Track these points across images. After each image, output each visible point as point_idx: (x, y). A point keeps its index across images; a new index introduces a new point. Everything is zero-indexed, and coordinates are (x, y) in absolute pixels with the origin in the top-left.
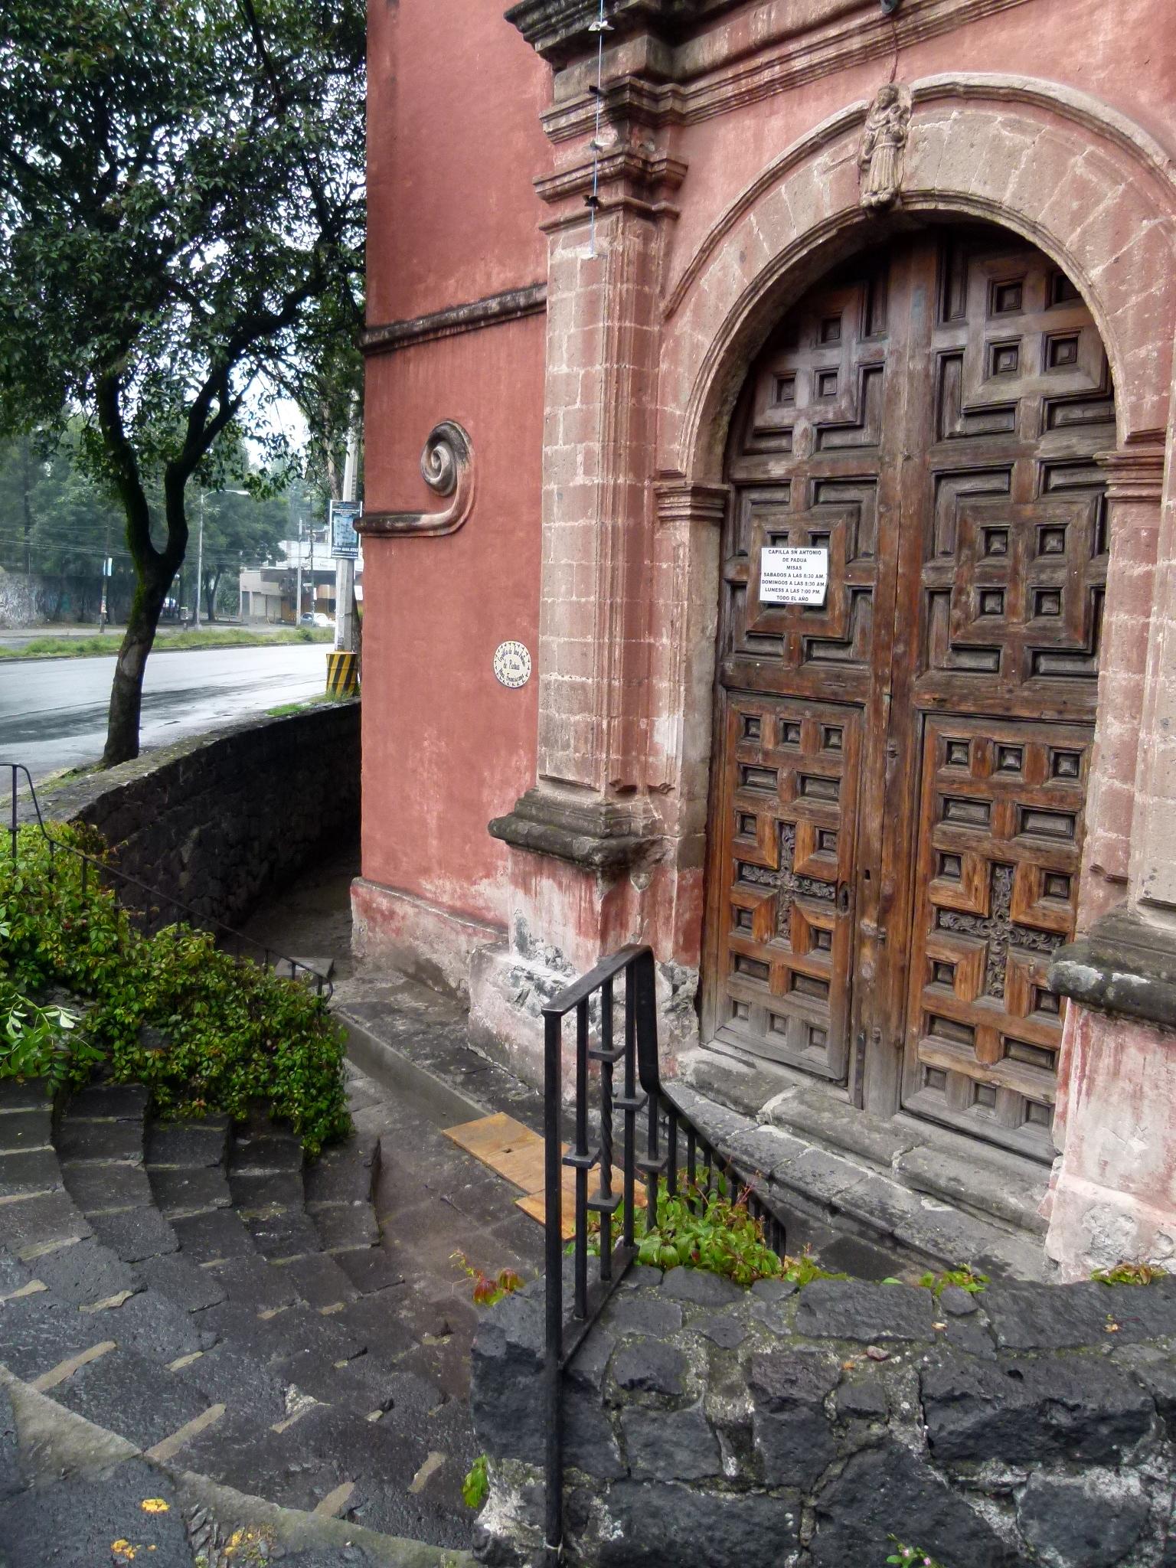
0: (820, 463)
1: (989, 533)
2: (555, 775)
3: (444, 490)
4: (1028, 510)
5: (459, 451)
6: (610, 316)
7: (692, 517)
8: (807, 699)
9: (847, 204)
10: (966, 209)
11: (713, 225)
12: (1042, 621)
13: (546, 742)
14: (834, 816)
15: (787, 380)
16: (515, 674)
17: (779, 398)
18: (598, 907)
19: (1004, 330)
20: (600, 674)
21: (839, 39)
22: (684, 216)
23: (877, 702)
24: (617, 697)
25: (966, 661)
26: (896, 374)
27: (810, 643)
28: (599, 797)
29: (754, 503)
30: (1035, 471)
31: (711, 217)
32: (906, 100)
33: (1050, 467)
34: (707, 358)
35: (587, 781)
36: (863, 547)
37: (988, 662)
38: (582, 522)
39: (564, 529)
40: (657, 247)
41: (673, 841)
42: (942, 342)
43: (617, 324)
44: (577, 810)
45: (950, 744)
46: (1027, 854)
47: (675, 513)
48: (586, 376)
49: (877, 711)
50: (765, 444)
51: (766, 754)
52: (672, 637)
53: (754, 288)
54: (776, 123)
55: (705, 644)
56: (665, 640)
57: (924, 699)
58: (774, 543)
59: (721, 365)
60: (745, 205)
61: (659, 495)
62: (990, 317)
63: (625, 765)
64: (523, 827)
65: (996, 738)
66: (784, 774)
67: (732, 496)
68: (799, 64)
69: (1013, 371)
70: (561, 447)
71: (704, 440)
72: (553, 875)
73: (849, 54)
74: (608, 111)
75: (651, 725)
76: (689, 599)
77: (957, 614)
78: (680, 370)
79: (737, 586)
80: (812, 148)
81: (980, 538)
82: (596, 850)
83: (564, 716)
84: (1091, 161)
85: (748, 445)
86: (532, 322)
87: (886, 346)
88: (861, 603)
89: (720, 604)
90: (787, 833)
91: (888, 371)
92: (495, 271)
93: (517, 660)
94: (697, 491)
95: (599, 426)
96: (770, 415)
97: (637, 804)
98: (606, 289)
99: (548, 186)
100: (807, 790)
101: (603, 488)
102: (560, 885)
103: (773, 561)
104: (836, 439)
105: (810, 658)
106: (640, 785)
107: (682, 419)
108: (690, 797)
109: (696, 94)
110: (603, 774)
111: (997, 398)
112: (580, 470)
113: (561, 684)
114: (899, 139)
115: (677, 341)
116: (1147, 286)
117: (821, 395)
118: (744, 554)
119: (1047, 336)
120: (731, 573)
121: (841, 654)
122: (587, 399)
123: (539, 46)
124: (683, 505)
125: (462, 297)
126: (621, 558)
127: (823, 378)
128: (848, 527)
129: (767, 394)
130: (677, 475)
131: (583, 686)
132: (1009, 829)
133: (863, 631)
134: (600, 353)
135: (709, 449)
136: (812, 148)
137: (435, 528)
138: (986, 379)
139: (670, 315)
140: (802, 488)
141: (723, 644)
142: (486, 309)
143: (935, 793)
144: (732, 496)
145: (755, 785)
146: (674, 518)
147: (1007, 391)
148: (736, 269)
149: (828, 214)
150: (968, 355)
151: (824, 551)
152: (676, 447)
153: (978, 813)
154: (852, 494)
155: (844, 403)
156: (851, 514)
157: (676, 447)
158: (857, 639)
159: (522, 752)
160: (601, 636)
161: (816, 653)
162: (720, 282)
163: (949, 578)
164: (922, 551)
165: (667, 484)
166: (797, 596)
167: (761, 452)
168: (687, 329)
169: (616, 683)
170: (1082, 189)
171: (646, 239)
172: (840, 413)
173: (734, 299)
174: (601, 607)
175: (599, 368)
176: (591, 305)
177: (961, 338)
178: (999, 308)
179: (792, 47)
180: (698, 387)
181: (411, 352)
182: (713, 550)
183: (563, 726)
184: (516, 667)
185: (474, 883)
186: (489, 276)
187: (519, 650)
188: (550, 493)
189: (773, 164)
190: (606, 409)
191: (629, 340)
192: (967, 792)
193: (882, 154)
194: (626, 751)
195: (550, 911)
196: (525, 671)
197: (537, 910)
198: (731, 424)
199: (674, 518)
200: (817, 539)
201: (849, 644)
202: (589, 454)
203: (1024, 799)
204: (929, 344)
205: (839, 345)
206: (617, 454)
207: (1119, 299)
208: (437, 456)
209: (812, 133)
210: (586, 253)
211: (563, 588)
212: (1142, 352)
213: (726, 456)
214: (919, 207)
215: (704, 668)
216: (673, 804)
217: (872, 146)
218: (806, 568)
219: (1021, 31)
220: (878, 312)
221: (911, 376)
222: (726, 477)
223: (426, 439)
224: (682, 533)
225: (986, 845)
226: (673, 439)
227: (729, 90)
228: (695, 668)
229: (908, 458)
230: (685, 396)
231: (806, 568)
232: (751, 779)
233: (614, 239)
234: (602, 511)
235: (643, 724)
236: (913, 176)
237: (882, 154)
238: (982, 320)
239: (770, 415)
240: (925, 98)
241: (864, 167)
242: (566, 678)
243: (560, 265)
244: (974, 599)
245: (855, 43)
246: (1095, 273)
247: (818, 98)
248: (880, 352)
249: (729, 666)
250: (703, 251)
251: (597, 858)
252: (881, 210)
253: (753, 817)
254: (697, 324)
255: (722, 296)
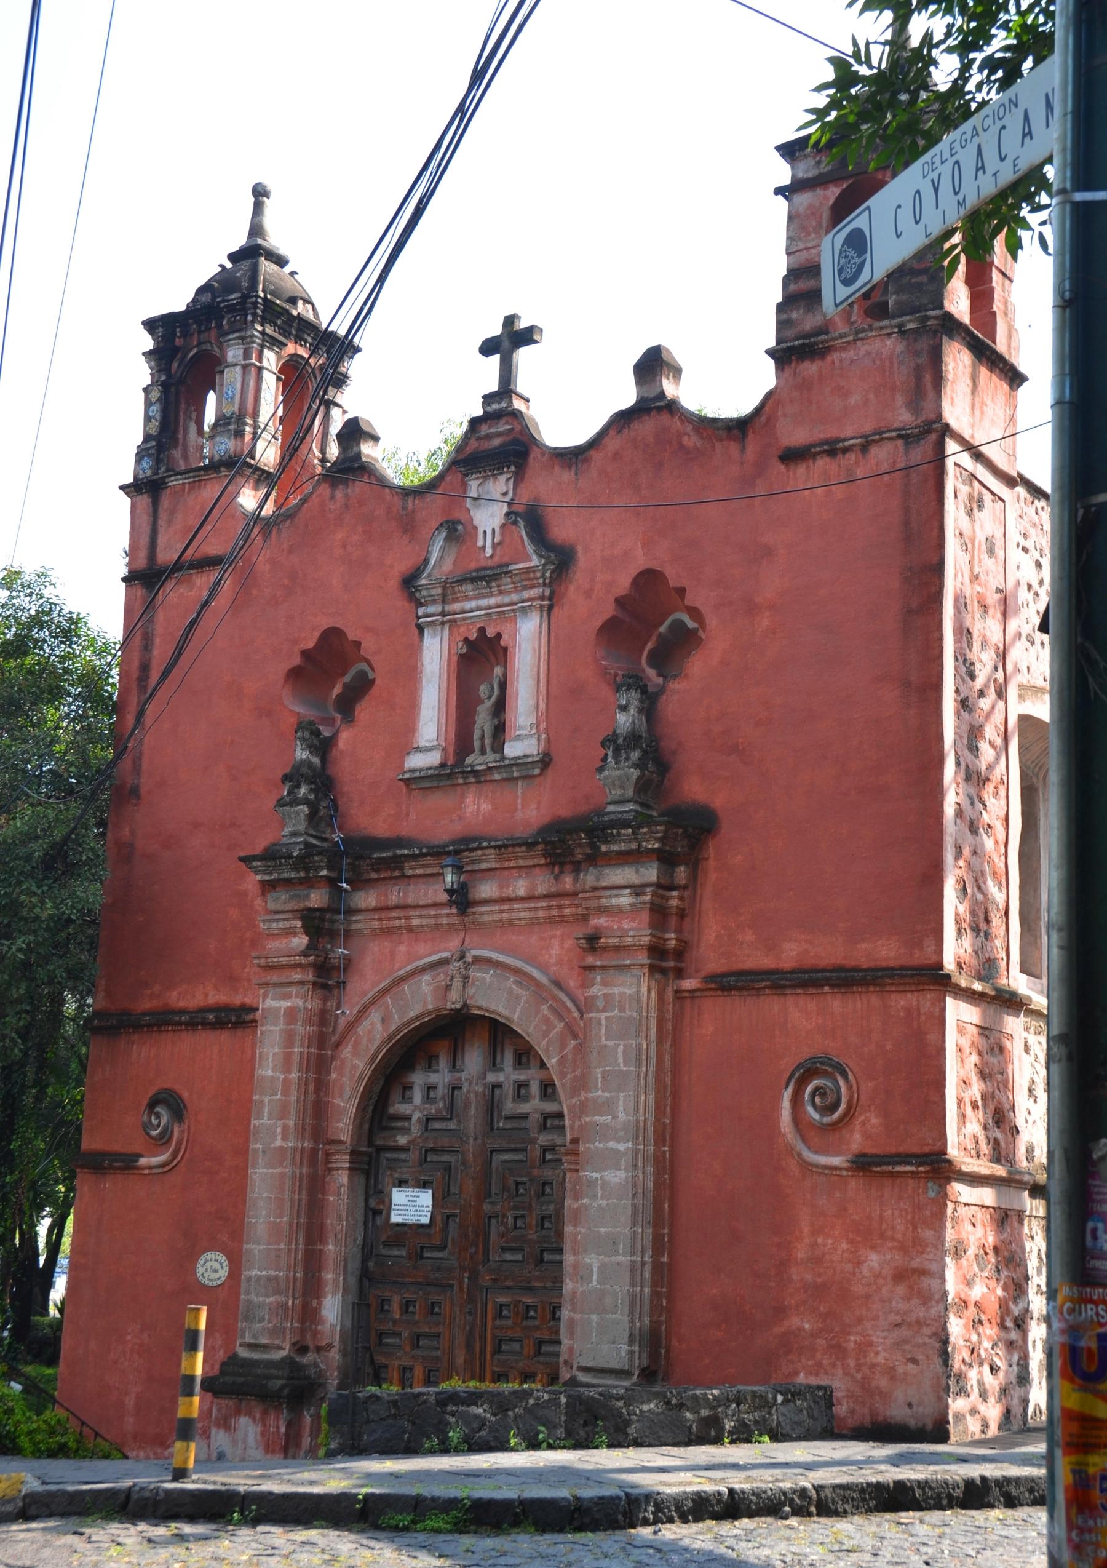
0: (427, 1138)
1: (517, 1184)
2: (252, 1341)
3: (164, 1139)
4: (535, 1172)
5: (178, 1111)
6: (302, 1045)
7: (350, 1169)
8: (419, 1284)
9: (440, 1004)
10: (498, 1018)
11: (365, 999)
12: (544, 1232)
13: (246, 1318)
14: (438, 1358)
15: (408, 1087)
16: (214, 1276)
17: (403, 1098)
18: (283, 1430)
19: (522, 1077)
20: (289, 1270)
21: (435, 916)
22: (349, 986)
23: (461, 1282)
24: (299, 1284)
25: (508, 1256)
26: (469, 1092)
27: (422, 1248)
28: (283, 1353)
29: (388, 1159)
30: (538, 1152)
31: (365, 993)
32: (469, 959)
33: (545, 1150)
34: (361, 1074)
35: (276, 1342)
36: (452, 1190)
37: (519, 1257)
38: (279, 1170)
39: (266, 1174)
40: (331, 1004)
41: (333, 1381)
42: (491, 1078)
43: (306, 1051)
44: (270, 1364)
45: (501, 1306)
46: (541, 1367)
47: (339, 1165)
48: (285, 1079)
49: (461, 1289)
50: (394, 1124)
51: (395, 1322)
52: (335, 1245)
53: (390, 1038)
54: (402, 948)
55: (355, 1249)
56: (331, 1247)
57: (486, 1279)
58: (400, 1186)
59: (370, 1078)
60: (385, 991)
61: (328, 1155)
62: (515, 1069)
63: (302, 1331)
64: (229, 1379)
65: (524, 1300)
66: (405, 1334)
67: (374, 1155)
68: (415, 922)
69: (526, 1099)
70: (265, 1121)
71: (358, 1121)
72: (249, 1414)
73: (442, 925)
74: (303, 926)
75: (320, 1304)
76: (347, 1220)
77: (502, 1229)
78: (344, 1079)
79: (376, 1212)
80: (423, 970)
81: (513, 1187)
82: (282, 1387)
83: (261, 1299)
84: (551, 1007)
85: (384, 1124)
86: (239, 1032)
87: (464, 1075)
88: (451, 1223)
89: (365, 1224)
90: (408, 1374)
91: (465, 1090)
92: (211, 993)
93: (217, 1266)
94: (353, 1153)
95: (293, 1112)
96: (399, 1108)
97: (309, 1358)
98: (300, 1029)
99: (263, 961)
100: (421, 1343)
101: (294, 1149)
102: (254, 1420)
103: (399, 1197)
104: (437, 1125)
105: (422, 1257)
106: (311, 1347)
107: (345, 1108)
108: (344, 1353)
109: (356, 921)
110: (288, 1337)
111: (519, 1111)
112: (279, 1137)
113: (259, 1278)
114: (466, 978)
115: (343, 1062)
116: (574, 1071)
117: (427, 1099)
118: (381, 1192)
119: (541, 1082)
120: (373, 1203)
121: (440, 1255)
122: (286, 1092)
123: (259, 877)
124: (344, 1161)
125: (182, 1004)
126: (304, 1192)
127: (429, 1088)
128: (444, 1178)
129: (396, 1094)
130: (342, 1142)
131: (276, 1278)
132: (532, 1353)
133: (453, 1239)
134: (295, 1067)
135: (361, 1126)
136: (423, 970)
137: (150, 1168)
138: (514, 1100)
139: (338, 1045)
140: (417, 1153)
141: (367, 1251)
142: (204, 1018)
143: (494, 1337)
144: (374, 1155)
145: (387, 1344)
146: (338, 1169)
147: (524, 1108)
148: (379, 1026)
149: (430, 1007)
150: (505, 1086)
151: (430, 1191)
152: (341, 1125)
153: (516, 1346)
154: (445, 1158)
155: (441, 1105)
156: (445, 1169)
157: (341, 1125)
158: (449, 1246)
159: (217, 1335)
160: (290, 1243)
161: (426, 1255)
162: (370, 1031)
163: (498, 1208)
164: (484, 1193)
165: (334, 1148)
166: (414, 1218)
167: (392, 1129)
168: (349, 1055)
169: (298, 1275)
170: (547, 1021)
171: (325, 1000)
172: (439, 1111)
173: (376, 1044)
174: (291, 1225)
175: (294, 1075)
176: (289, 1039)
177: (501, 1077)
178: (520, 1064)
179: (412, 913)
180: (354, 1090)
181: (136, 1037)
182: (361, 1191)
183: (261, 1306)
184: (216, 1271)
185: (169, 1447)
186: (206, 995)
187: (219, 1258)
188: (256, 1151)
189: (401, 972)
190: (298, 1101)
191: (313, 1058)
192: (510, 1334)
193: (457, 984)
194: (303, 1321)
195: (245, 1441)
196: (223, 1273)
197: (234, 1442)
198: (374, 1111)
199: (338, 1169)
200: (424, 1185)
201: (445, 1247)
202: (285, 1128)
203: (538, 1335)
204: (485, 1078)
205: (437, 1071)
206: (304, 1129)
207: (563, 1075)
208: (158, 1116)
209: (422, 962)
210: (286, 1004)
211: (264, 1213)
212: (574, 1101)
213: (371, 1130)
214: (476, 1012)
215: (355, 1265)
216: (333, 1357)
217: (452, 979)
218: (419, 1201)
219: (521, 938)
220: (459, 1056)
221: (476, 1094)
222: (370, 1143)
223: (145, 1102)
224: (343, 1178)
225: (521, 1364)
226: (339, 1121)
227: (376, 924)
228: (349, 1265)
229: (475, 1139)
230: (347, 1095)
231: (419, 1201)
232: (385, 1340)
233: (306, 1001)
234: (293, 1163)
235: (314, 1303)
236: (472, 998)
237: (457, 984)
238: (511, 1069)
239: (399, 1108)
240: (477, 960)
241: (448, 987)
242: (264, 1273)
243: (269, 1009)
244: (510, 1220)
245: (444, 921)
246: (554, 1060)
247: (425, 942)
248: (460, 1079)
249: (371, 1264)
250: (359, 1012)
251: (286, 1392)
252: (458, 1011)
253: (386, 1367)
254: (355, 1054)
255: (370, 1040)
